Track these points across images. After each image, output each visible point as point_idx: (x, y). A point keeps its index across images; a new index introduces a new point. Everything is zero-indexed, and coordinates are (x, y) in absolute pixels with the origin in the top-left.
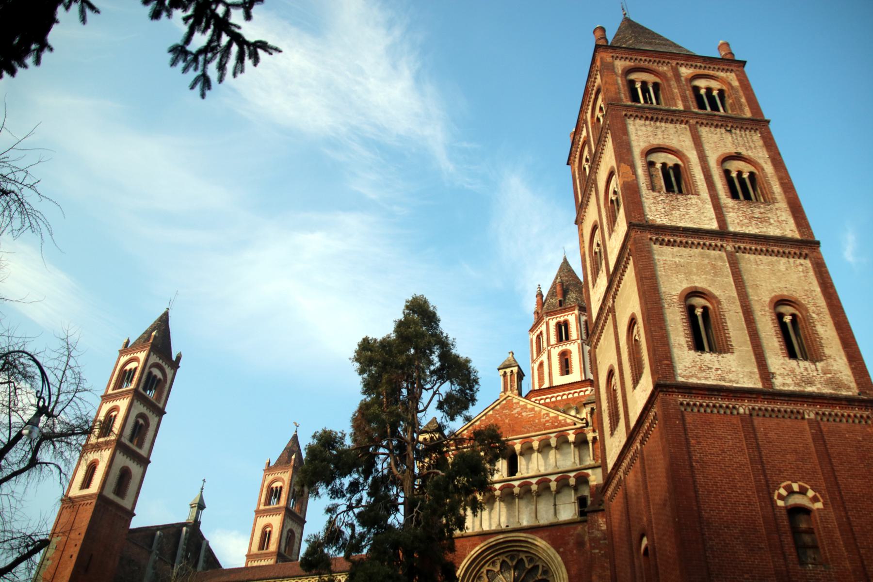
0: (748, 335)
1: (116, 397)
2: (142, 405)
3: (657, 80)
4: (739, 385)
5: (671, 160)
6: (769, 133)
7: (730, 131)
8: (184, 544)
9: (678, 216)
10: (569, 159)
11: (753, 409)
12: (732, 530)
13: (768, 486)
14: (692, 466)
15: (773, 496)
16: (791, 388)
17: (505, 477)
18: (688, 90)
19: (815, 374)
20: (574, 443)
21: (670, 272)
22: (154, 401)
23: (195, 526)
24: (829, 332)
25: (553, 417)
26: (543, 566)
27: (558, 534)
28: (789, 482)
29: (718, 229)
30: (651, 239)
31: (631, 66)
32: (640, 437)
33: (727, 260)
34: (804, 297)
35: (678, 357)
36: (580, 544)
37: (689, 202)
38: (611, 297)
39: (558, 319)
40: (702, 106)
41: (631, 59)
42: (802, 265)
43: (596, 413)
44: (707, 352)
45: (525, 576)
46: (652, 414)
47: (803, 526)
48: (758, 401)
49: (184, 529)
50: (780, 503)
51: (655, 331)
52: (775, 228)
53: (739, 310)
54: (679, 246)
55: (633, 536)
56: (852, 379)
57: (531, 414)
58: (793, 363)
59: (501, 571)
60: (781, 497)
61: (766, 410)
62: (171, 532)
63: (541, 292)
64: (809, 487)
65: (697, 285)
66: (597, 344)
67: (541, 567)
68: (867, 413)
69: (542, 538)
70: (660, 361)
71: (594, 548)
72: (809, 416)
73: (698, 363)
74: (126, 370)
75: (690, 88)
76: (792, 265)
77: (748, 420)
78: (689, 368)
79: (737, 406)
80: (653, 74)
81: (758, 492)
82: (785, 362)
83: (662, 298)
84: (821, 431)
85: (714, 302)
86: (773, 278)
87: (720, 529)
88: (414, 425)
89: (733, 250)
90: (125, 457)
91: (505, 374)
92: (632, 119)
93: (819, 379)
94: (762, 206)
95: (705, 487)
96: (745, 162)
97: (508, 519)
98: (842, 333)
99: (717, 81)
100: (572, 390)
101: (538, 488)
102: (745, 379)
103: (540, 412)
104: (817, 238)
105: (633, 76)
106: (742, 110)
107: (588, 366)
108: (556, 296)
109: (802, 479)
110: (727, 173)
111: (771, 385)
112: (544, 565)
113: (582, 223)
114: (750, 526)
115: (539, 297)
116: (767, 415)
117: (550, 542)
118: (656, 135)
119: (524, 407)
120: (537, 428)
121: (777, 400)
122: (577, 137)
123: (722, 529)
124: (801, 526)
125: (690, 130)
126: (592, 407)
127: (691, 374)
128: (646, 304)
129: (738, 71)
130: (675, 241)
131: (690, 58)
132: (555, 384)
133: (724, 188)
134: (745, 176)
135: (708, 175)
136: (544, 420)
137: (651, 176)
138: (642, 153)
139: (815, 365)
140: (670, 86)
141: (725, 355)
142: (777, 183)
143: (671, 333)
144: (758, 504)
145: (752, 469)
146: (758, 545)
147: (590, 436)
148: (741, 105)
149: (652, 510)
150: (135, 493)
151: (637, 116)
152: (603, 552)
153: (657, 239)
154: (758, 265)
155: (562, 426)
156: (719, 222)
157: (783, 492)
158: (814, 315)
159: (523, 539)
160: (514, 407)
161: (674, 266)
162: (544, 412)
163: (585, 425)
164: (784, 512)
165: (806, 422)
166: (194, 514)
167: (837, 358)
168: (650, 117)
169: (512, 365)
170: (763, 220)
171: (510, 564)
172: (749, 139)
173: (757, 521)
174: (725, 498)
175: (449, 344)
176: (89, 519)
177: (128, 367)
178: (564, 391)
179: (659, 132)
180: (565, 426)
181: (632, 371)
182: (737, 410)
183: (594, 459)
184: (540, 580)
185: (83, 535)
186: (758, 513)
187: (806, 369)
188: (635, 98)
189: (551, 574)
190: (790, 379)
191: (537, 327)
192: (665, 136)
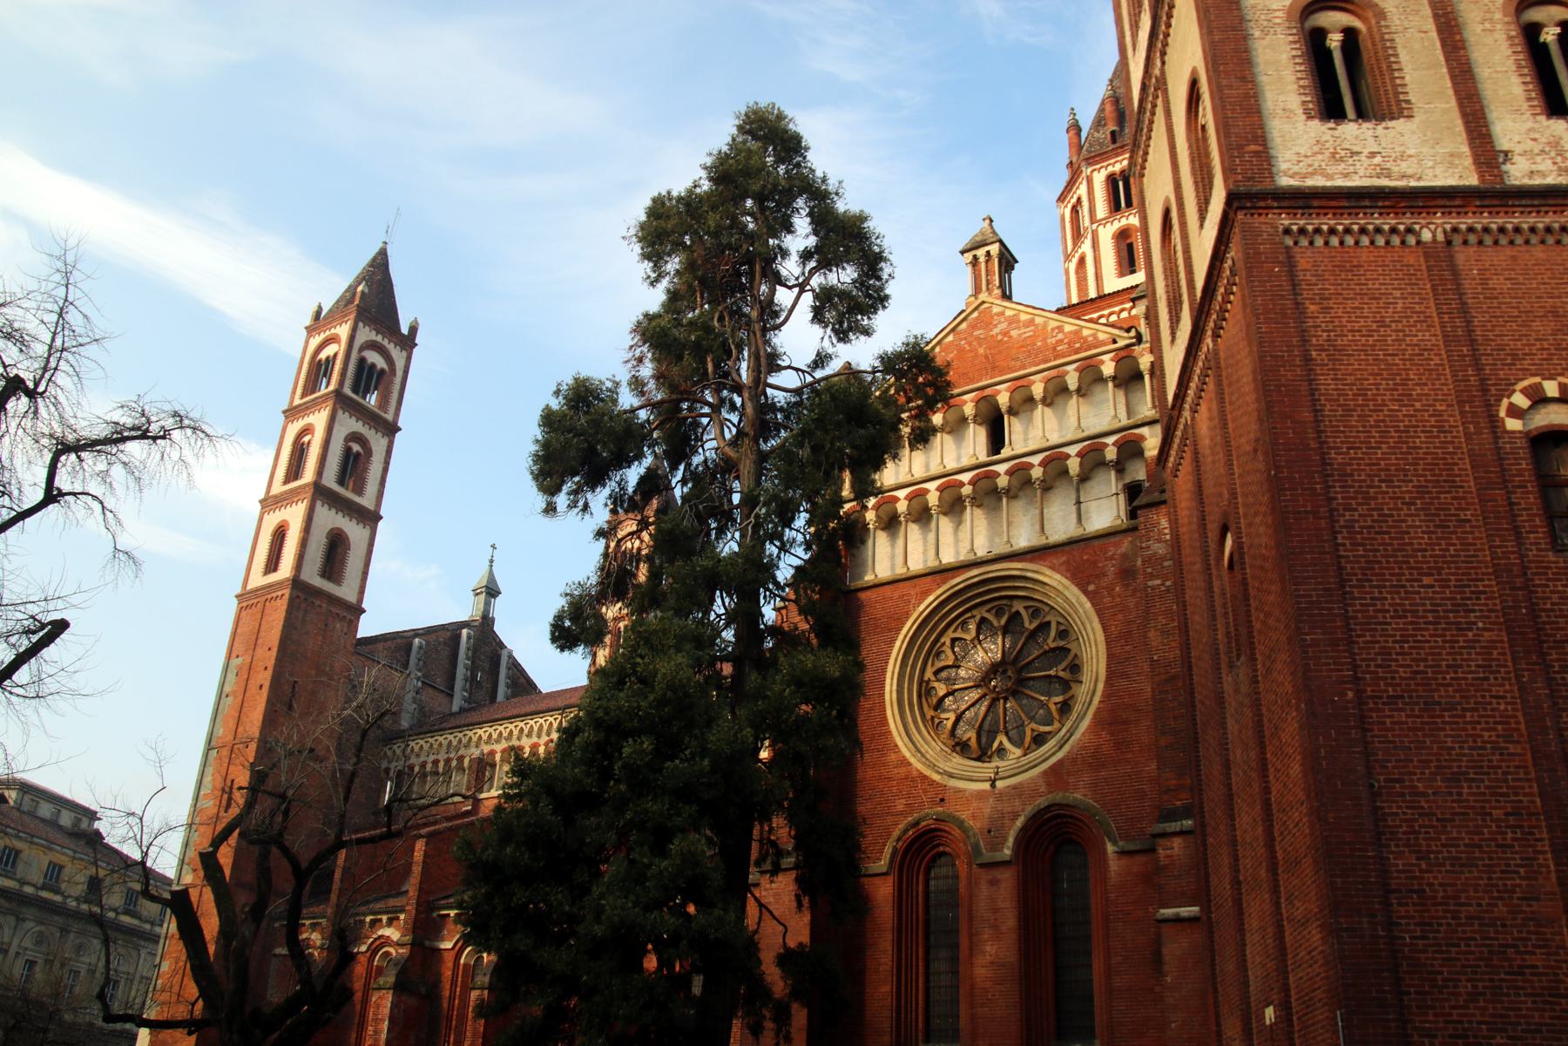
0: (1447, 77)
1: (307, 408)
2: (354, 419)
4: (1422, 184)
8: (468, 659)
11: (1455, 230)
12: (1400, 487)
13: (1485, 391)
14: (1307, 359)
15: (1498, 411)
17: (983, 457)
20: (1114, 378)
22: (376, 410)
23: (485, 625)
25: (1070, 333)
26: (1058, 623)
27: (1085, 558)
28: (1537, 379)
32: (1212, 324)
35: (1283, 136)
38: (1158, 54)
39: (1110, 169)
43: (1151, 317)
44: (1350, 121)
45: (1024, 644)
48: (1466, 213)
49: (465, 632)
50: (1513, 424)
51: (1230, 87)
53: (1430, 25)
55: (1210, 535)
59: (977, 640)
60: (1514, 412)
61: (1486, 230)
62: (441, 640)
63: (1077, 121)
67: (1053, 625)
69: (1052, 568)
70: (1240, 147)
73: (1327, 145)
74: (320, 361)
77: (1441, 256)
78: (1306, 157)
79: (1417, 227)
81: (1461, 403)
83: (1248, 18)
85: (1370, 14)
87: (1368, 487)
88: (770, 362)
90: (334, 511)
91: (975, 262)
97: (991, 540)
101: (1044, 472)
103: (1045, 324)
111: (1501, 175)
114: (1441, 475)
115: (1072, 132)
116: (1488, 240)
117: (1068, 575)
120: (1041, 357)
121: (1514, 206)
124: (1562, 472)
127: (1310, 170)
128: (1210, 33)
132: (1107, 291)
143: (1267, 88)
144: (1461, 429)
145: (1448, 356)
146: (1459, 515)
149: (1236, 470)
150: (360, 573)
152: (1168, 583)
157: (1520, 400)
160: (995, 323)
162: (1053, 324)
166: (481, 606)
169: (988, 241)
171: (995, 623)
173: (1457, 464)
174: (1383, 421)
175: (830, 193)
176: (282, 623)
177: (323, 355)
178: (1122, 303)
180: (1096, 347)
181: (1197, 192)
182: (1417, 234)
184: (1053, 650)
185: (275, 650)
186: (1460, 448)
189: (1074, 637)
191: (1071, 190)
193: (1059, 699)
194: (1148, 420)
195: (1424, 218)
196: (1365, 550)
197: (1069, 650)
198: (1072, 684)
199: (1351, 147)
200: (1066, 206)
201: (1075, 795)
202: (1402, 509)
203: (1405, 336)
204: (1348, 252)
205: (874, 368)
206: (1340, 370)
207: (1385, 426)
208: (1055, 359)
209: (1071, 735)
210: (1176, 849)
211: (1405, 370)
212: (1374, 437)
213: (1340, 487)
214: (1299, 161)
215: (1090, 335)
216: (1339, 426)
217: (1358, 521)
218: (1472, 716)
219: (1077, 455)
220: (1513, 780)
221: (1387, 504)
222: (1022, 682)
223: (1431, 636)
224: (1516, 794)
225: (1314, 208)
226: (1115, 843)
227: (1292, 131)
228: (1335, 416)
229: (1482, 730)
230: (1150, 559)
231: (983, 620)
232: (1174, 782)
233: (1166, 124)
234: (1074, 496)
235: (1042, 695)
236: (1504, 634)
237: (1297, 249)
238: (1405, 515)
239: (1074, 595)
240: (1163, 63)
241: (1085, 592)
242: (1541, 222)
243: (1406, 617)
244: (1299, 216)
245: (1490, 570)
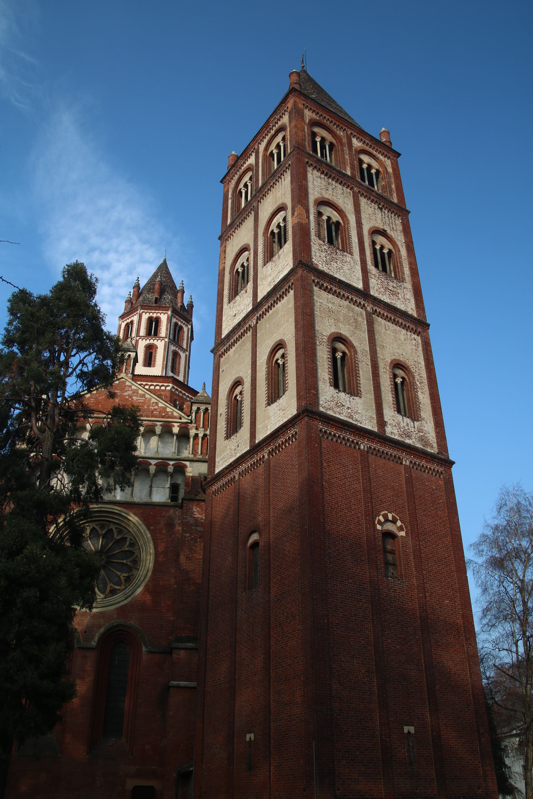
3: (334, 141)
4: (362, 425)
5: (336, 217)
6: (408, 222)
7: (381, 209)
9: (335, 268)
10: (224, 178)
11: (370, 447)
12: (345, 543)
16: (396, 437)
18: (356, 161)
19: (413, 430)
20: (177, 435)
21: (324, 314)
24: (425, 399)
25: (161, 407)
26: (131, 539)
27: (151, 513)
28: (387, 512)
29: (362, 289)
30: (314, 281)
31: (316, 119)
32: (270, 448)
33: (365, 318)
34: (413, 366)
36: (170, 525)
37: (344, 259)
39: (151, 314)
40: (363, 179)
41: (318, 113)
42: (415, 340)
46: (291, 433)
47: (389, 547)
50: (379, 527)
51: (308, 363)
52: (402, 303)
53: (369, 363)
54: (333, 294)
56: (435, 440)
57: (141, 400)
58: (400, 417)
60: (380, 523)
64: (398, 518)
65: (342, 332)
66: (223, 354)
67: (128, 540)
68: (441, 469)
69: (135, 514)
70: (309, 390)
72: (406, 462)
73: (335, 399)
75: (358, 160)
76: (409, 337)
77: (364, 455)
79: (360, 443)
80: (331, 134)
82: (394, 415)
84: (411, 476)
86: (395, 344)
87: (336, 541)
89: (371, 311)
92: (312, 168)
93: (415, 435)
94: (395, 281)
95: (330, 504)
96: (388, 239)
98: (434, 403)
99: (377, 162)
100: (154, 382)
102: (367, 422)
104: (428, 322)
105: (316, 130)
106: (391, 195)
107: (170, 364)
108: (153, 292)
109: (395, 511)
110: (374, 243)
111: (384, 431)
112: (132, 538)
113: (227, 240)
114: (357, 541)
115: (135, 289)
117: (142, 519)
118: (327, 190)
119: (135, 392)
121: (387, 444)
122: (241, 162)
123: (337, 541)
125: (353, 196)
126: (199, 406)
127: (329, 407)
129: (393, 159)
130: (331, 289)
131: (361, 133)
133: (371, 256)
134: (385, 251)
135: (362, 241)
136: (153, 408)
137: (319, 224)
138: (315, 201)
139: (414, 423)
140: (343, 150)
141: (355, 398)
142: (408, 266)
143: (319, 367)
145: (363, 496)
146: (361, 558)
147: (193, 432)
148: (391, 190)
151: (316, 167)
152: (192, 536)
153: (318, 282)
154: (386, 330)
155: (168, 417)
156: (364, 284)
158: (418, 383)
159: (118, 512)
160: (126, 389)
161: (327, 310)
162: (153, 400)
163: (190, 421)
164: (380, 535)
165: (403, 466)
167: (428, 422)
168: (325, 172)
170: (395, 294)
171: (100, 532)
172: (393, 221)
173: (362, 538)
178: (147, 381)
179: (330, 188)
180: (172, 418)
183: (193, 453)
187: (407, 425)
188: (315, 150)
190: (397, 430)
192: (334, 194)
194: (190, 459)
195: (362, 440)
196: (333, 565)
197: (134, 553)
198: (134, 570)
199: (342, 403)
200: (124, 322)
202: (345, 552)
203: (351, 484)
204: (338, 445)
205: (110, 413)
206: (331, 492)
207: (343, 518)
208: (152, 417)
209: (132, 593)
210: (181, 656)
211: (350, 497)
212: (339, 522)
213: (328, 539)
214: (326, 402)
215: (171, 412)
216: (329, 514)
217: (332, 553)
218: (359, 634)
219: (155, 465)
220: (369, 659)
221: (341, 549)
223: (350, 602)
224: (369, 665)
225: (330, 424)
226: (147, 647)
227: (325, 389)
228: (328, 510)
229: (362, 640)
234: (149, 484)
235: (117, 571)
236: (370, 605)
237: (322, 438)
238: (346, 554)
239: (143, 529)
240: (257, 323)
241: (149, 529)
242: (395, 453)
243: (343, 594)
244: (325, 425)
245: (368, 581)
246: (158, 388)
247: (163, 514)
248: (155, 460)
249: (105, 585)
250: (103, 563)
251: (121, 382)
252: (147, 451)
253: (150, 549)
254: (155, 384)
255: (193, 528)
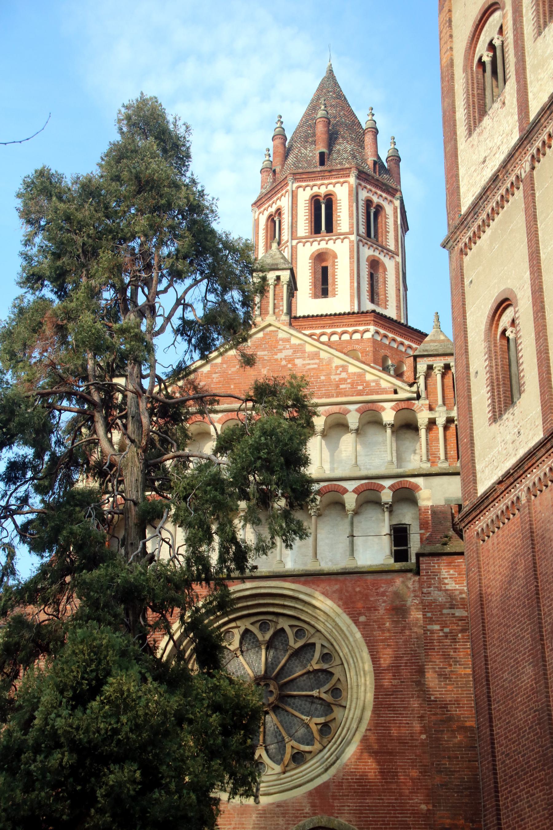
26: (323, 646)
27: (358, 589)
39: (316, 189)
57: (313, 364)
67: (318, 647)
71: (431, 621)
100: (338, 327)
108: (314, 143)
112: (326, 644)
115: (278, 141)
117: (341, 603)
119: (299, 350)
120: (323, 390)
126: (430, 363)
136: (337, 378)
147: (423, 417)
152: (447, 630)
160: (280, 347)
162: (337, 362)
169: (279, 267)
178: (323, 327)
180: (377, 393)
183: (428, 460)
184: (316, 671)
191: (270, 198)
193: (321, 720)
194: (424, 472)
197: (332, 674)
198: (335, 709)
200: (262, 213)
201: (339, 819)
208: (337, 396)
209: (337, 759)
215: (374, 381)
219: (354, 491)
222: (283, 698)
230: (430, 604)
231: (247, 631)
232: (448, 821)
233: (529, 228)
234: (347, 532)
235: (302, 713)
239: (345, 623)
241: (356, 622)
246: (346, 337)
247: (382, 590)
248: (353, 482)
249: (281, 743)
250: (271, 699)
251: (267, 334)
252: (335, 466)
253: (363, 663)
254: (339, 330)
255: (445, 611)
